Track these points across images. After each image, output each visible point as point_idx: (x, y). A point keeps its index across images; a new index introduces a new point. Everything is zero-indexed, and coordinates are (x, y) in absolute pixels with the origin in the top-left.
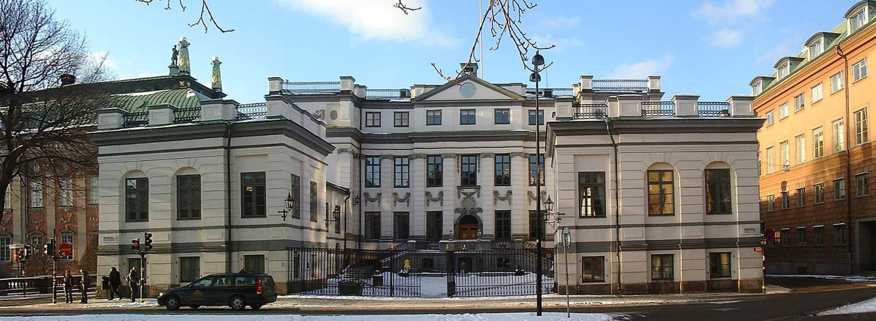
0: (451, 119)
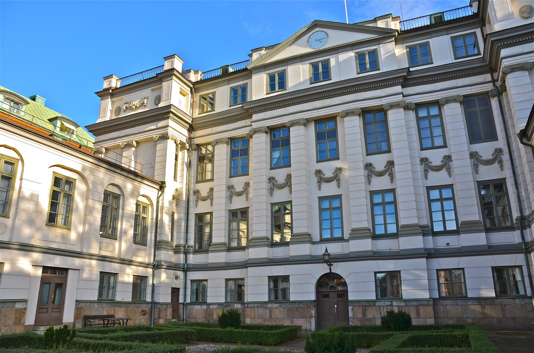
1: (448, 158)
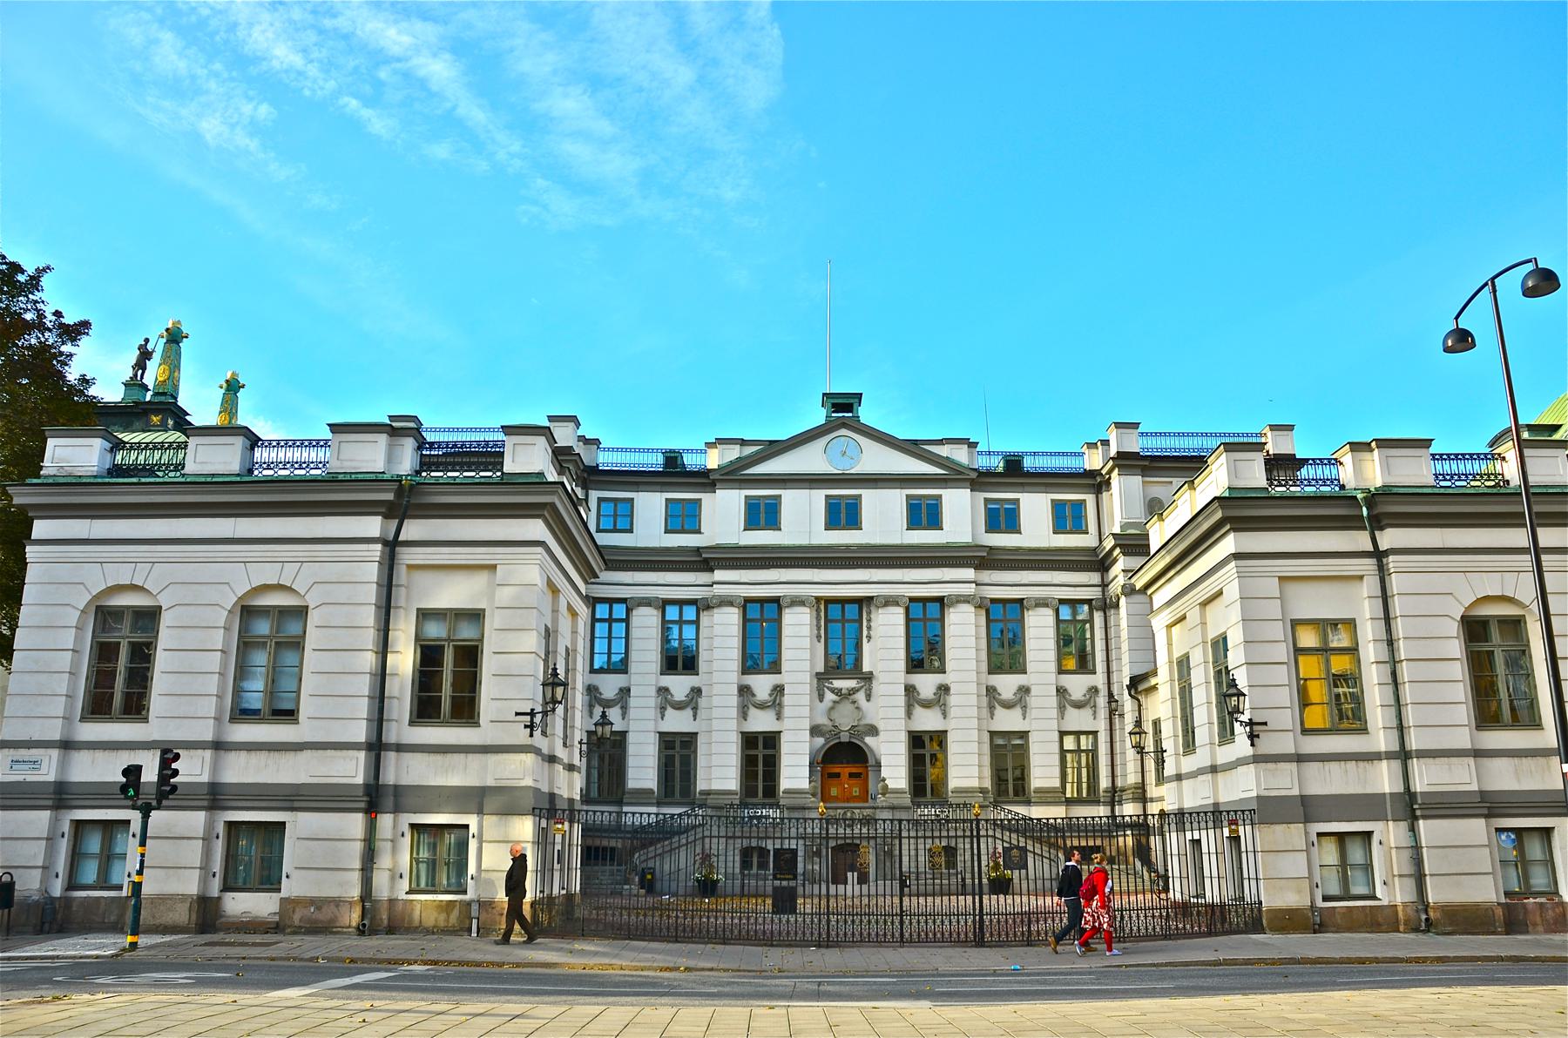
0: (803, 521)
1: (1024, 690)
